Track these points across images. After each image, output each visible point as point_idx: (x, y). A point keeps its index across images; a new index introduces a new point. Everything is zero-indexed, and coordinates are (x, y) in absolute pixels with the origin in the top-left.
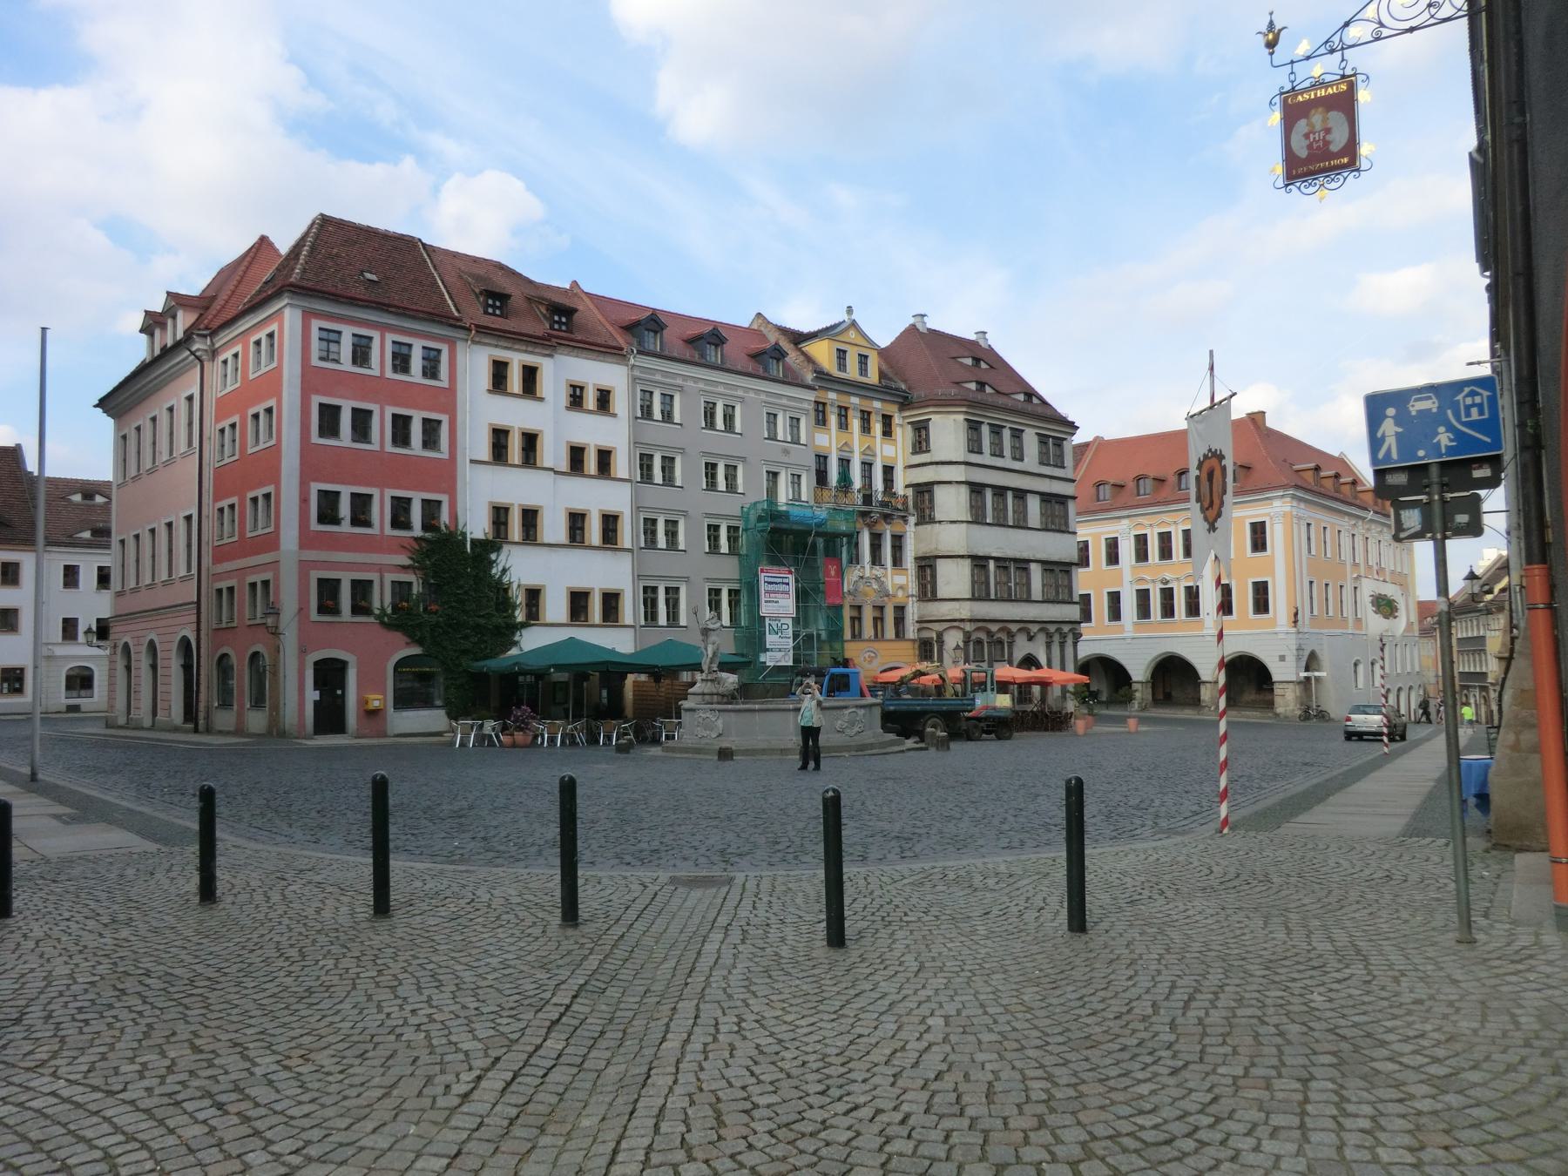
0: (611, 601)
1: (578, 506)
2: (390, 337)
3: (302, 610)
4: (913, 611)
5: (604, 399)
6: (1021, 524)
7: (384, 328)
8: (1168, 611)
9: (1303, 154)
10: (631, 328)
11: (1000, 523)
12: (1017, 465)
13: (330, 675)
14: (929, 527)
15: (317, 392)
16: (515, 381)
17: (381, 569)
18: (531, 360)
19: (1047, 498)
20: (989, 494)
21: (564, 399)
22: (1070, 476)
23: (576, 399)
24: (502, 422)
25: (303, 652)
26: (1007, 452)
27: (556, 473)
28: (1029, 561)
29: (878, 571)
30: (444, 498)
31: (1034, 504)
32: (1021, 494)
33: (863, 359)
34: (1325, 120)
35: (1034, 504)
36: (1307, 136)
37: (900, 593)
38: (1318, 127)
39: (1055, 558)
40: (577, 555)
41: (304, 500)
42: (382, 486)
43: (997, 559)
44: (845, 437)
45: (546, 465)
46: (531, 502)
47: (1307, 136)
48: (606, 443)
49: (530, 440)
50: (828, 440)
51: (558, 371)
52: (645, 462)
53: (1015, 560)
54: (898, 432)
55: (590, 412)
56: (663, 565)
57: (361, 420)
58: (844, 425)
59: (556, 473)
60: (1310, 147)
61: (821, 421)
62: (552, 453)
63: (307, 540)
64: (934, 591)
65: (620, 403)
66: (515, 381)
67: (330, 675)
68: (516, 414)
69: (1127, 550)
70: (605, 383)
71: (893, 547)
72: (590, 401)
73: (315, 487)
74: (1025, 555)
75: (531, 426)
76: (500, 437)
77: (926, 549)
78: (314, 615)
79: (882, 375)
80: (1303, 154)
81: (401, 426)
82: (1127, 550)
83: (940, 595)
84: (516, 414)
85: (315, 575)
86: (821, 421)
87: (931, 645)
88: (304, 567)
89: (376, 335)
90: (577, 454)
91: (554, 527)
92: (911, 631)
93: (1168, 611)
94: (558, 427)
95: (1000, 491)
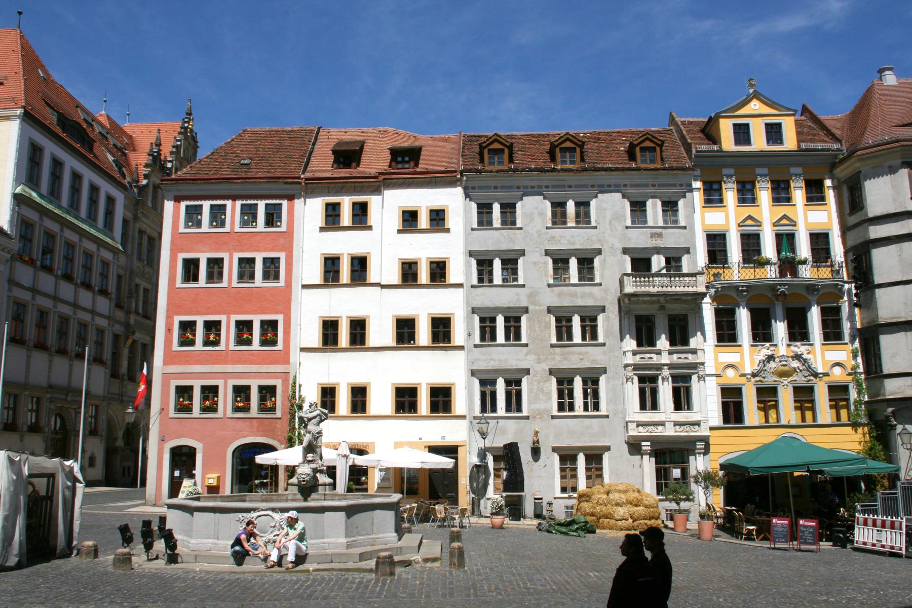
2: (239, 203)
7: (234, 198)
15: (182, 251)
16: (346, 218)
17: (226, 375)
21: (396, 222)
25: (163, 440)
27: (383, 287)
29: (800, 348)
30: (280, 318)
37: (837, 371)
40: (406, 357)
41: (169, 330)
42: (228, 313)
45: (372, 281)
46: (358, 313)
59: (383, 287)
63: (170, 358)
64: (881, 371)
66: (346, 218)
68: (346, 244)
73: (177, 319)
78: (172, 413)
79: (800, 139)
84: (346, 244)
88: (167, 377)
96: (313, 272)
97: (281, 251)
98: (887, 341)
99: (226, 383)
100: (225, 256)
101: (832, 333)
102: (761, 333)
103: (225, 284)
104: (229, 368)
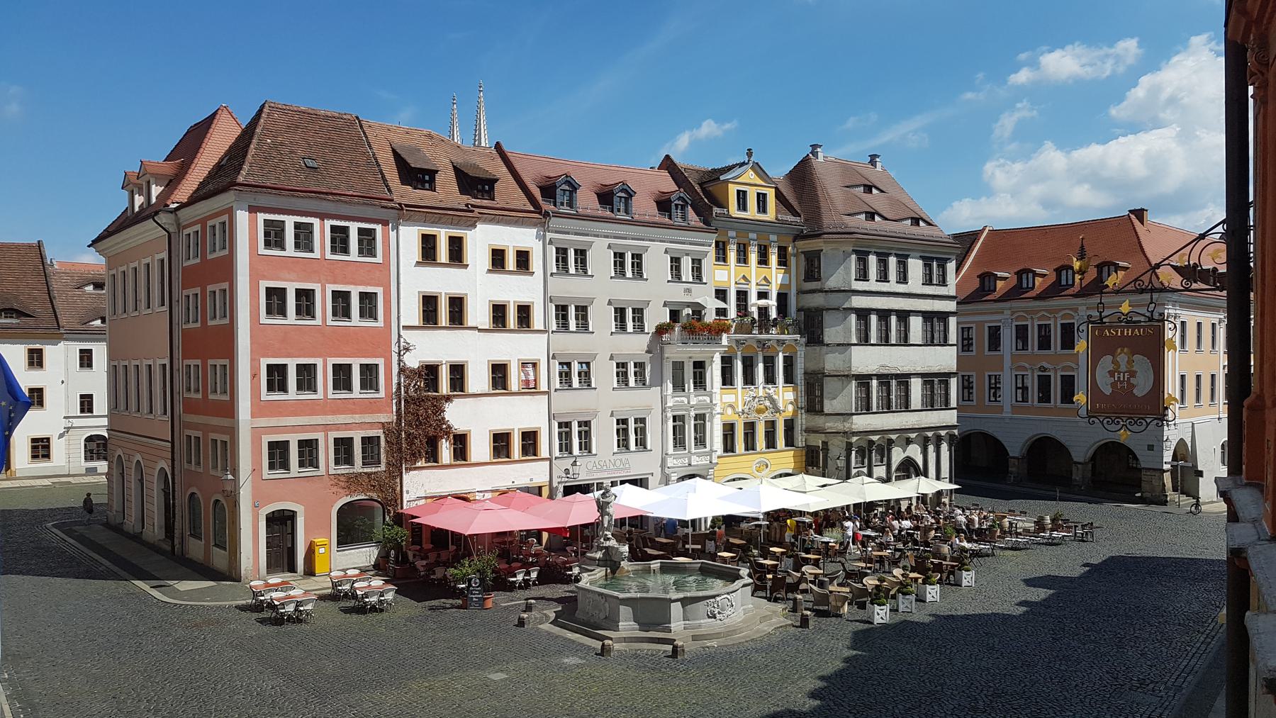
0: (530, 439)
1: (499, 358)
2: (328, 223)
3: (256, 470)
4: (802, 421)
5: (523, 259)
6: (904, 341)
7: (322, 216)
8: (1045, 396)
9: (1108, 391)
10: (549, 190)
11: (885, 341)
12: (901, 288)
13: (281, 523)
14: (818, 348)
16: (443, 253)
17: (326, 428)
18: (456, 232)
19: (928, 316)
20: (874, 318)
22: (953, 293)
23: (498, 258)
24: (430, 289)
25: (256, 507)
26: (893, 274)
27: (480, 330)
28: (909, 376)
29: (771, 390)
31: (916, 324)
32: (904, 316)
33: (762, 198)
34: (1130, 362)
35: (916, 324)
36: (1112, 374)
38: (1123, 368)
39: (935, 370)
41: (255, 376)
42: (324, 357)
43: (879, 376)
44: (743, 270)
45: (470, 324)
46: (457, 359)
47: (1112, 374)
48: (524, 300)
49: (457, 305)
50: (725, 275)
51: (481, 239)
52: (562, 311)
53: (897, 376)
54: (793, 261)
55: (511, 272)
56: (573, 402)
57: (306, 300)
58: (743, 258)
59: (480, 330)
60: (1114, 385)
61: (722, 257)
62: (478, 314)
63: (259, 409)
65: (536, 263)
66: (443, 253)
67: (281, 523)
68: (443, 281)
69: (1008, 336)
70: (523, 246)
71: (785, 368)
72: (511, 262)
73: (264, 362)
74: (906, 369)
75: (456, 291)
76: (429, 302)
77: (812, 367)
80: (1108, 391)
81: (341, 299)
82: (1008, 336)
83: (826, 411)
84: (443, 281)
85: (266, 439)
86: (722, 257)
87: (818, 453)
88: (257, 433)
89: (316, 222)
90: (499, 312)
91: (478, 379)
92: (800, 440)
93: (1045, 396)
94: (479, 286)
95: (884, 315)
96: (411, 312)
97: (378, 285)
98: (829, 385)
99: (326, 437)
100: (316, 287)
101: (789, 379)
102: (749, 379)
103: (318, 321)
104: (329, 419)
